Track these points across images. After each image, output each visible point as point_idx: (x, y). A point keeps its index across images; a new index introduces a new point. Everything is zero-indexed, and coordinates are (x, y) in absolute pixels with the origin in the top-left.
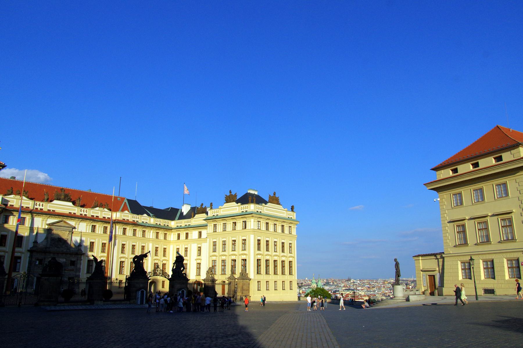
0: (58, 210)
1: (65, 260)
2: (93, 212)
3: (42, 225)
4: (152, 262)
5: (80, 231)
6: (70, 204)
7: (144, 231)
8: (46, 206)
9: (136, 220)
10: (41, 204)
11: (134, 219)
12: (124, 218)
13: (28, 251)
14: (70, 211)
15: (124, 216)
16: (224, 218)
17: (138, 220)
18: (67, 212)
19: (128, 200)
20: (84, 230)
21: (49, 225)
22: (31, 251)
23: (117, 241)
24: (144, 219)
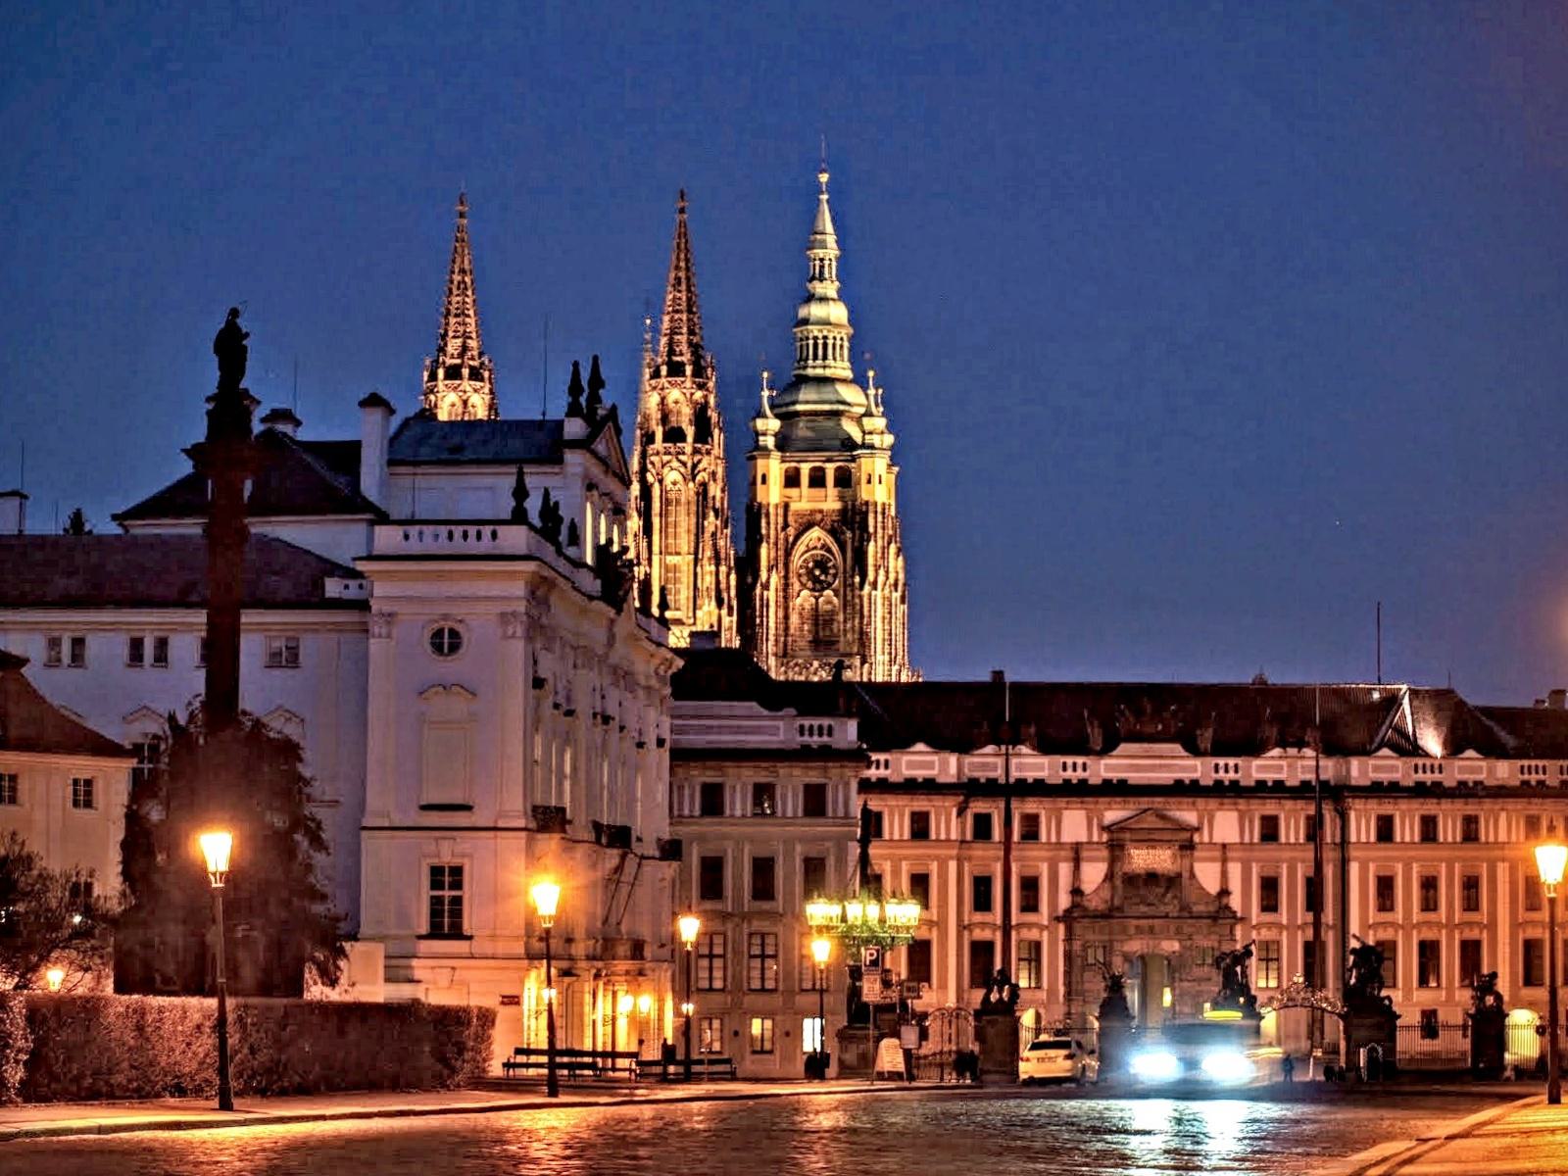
0: (1134, 778)
1: (1176, 946)
2: (1261, 768)
3: (1090, 834)
4: (1513, 936)
5: (1218, 838)
6: (1177, 748)
8: (1102, 769)
10: (1080, 760)
11: (1420, 777)
13: (1058, 919)
18: (1165, 777)
20: (1232, 837)
22: (1068, 918)
23: (1354, 869)
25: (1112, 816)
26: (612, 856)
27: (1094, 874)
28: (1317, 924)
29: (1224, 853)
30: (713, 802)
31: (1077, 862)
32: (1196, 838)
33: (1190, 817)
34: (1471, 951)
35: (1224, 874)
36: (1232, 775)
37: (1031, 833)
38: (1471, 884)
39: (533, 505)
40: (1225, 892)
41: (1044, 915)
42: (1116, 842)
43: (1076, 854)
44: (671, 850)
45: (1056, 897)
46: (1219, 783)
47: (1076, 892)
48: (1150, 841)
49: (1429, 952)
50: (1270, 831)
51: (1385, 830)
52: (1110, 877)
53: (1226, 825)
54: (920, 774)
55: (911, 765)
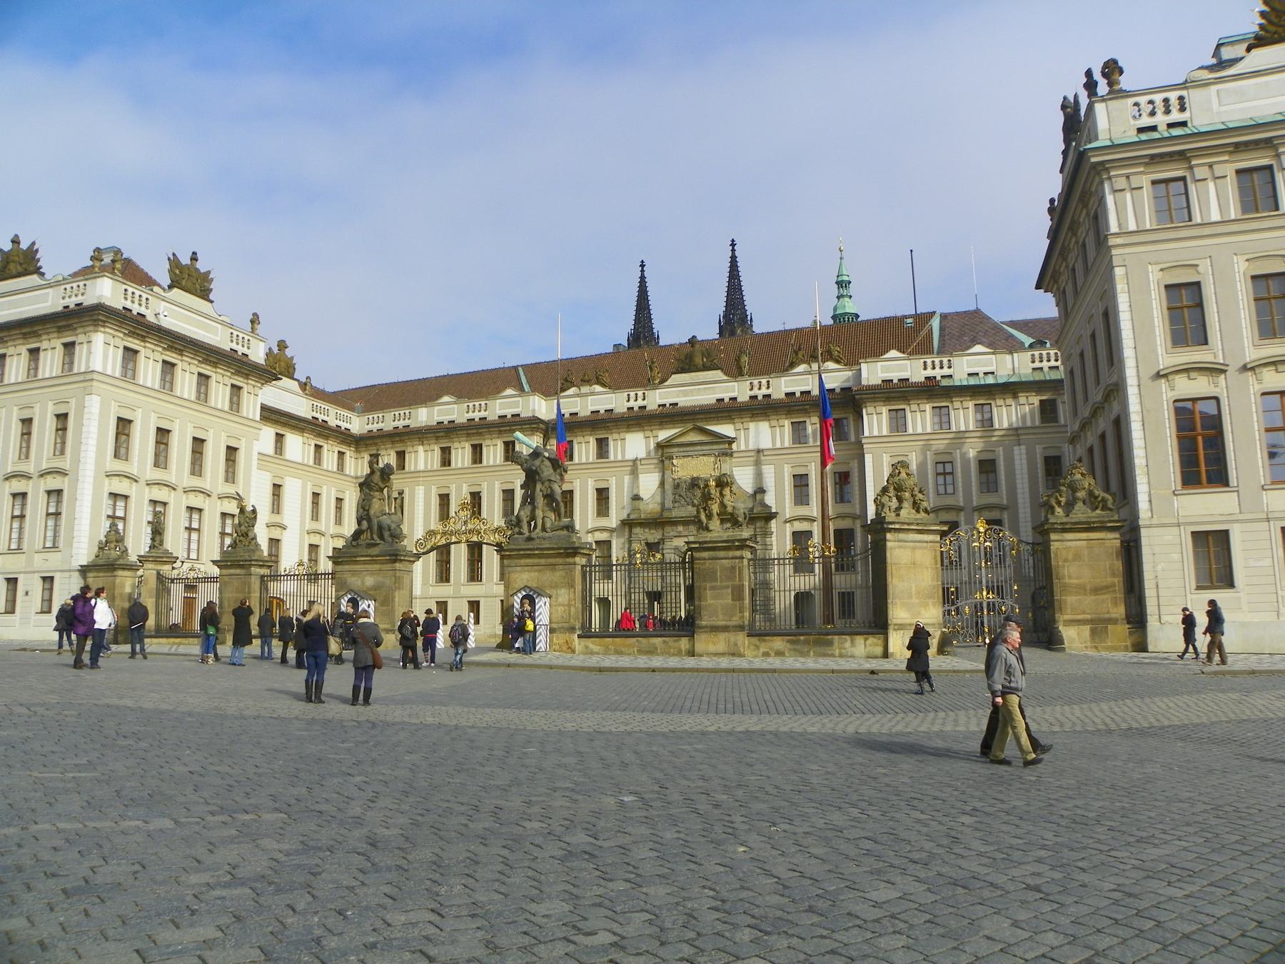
6: (718, 374)
8: (656, 398)
9: (938, 373)
11: (930, 373)
12: (888, 376)
14: (720, 396)
15: (885, 370)
17: (946, 371)
19: (944, 317)
20: (766, 443)
21: (660, 446)
23: (868, 459)
25: (664, 435)
27: (649, 484)
29: (758, 457)
31: (634, 472)
32: (734, 446)
33: (726, 429)
35: (759, 476)
36: (764, 391)
40: (760, 491)
41: (613, 521)
43: (634, 467)
46: (754, 398)
51: (898, 423)
52: (662, 484)
53: (762, 434)
54: (509, 412)
55: (502, 406)
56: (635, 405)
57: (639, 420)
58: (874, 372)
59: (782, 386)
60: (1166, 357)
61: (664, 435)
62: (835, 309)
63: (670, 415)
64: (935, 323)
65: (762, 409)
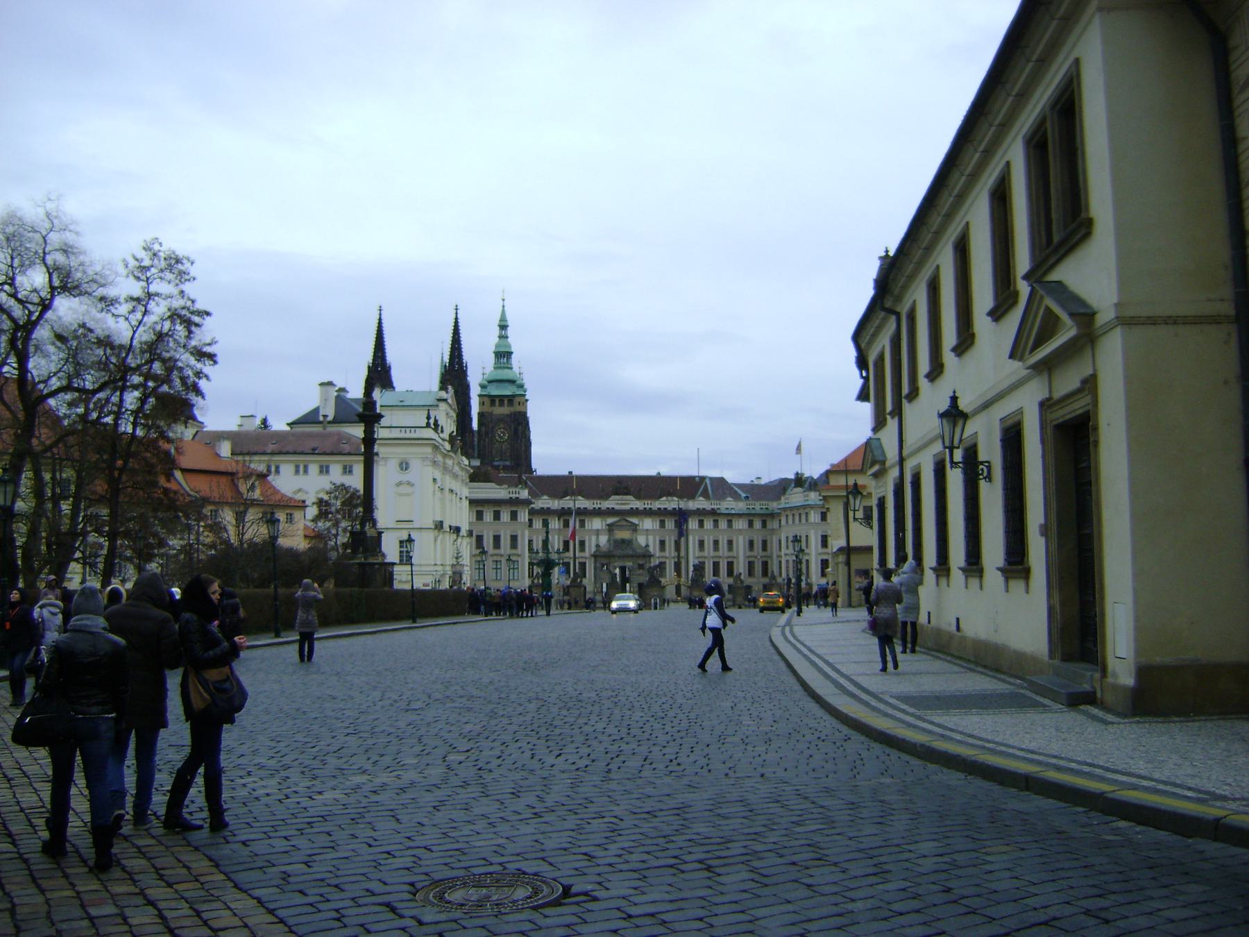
0: (617, 507)
7: (730, 522)
16: (791, 508)
18: (627, 507)
19: (711, 479)
22: (595, 556)
23: (691, 538)
24: (728, 505)
26: (454, 536)
27: (603, 539)
28: (679, 557)
30: (480, 516)
34: (730, 565)
37: (582, 523)
38: (730, 543)
39: (432, 421)
40: (647, 546)
41: (587, 554)
42: (611, 528)
43: (598, 532)
44: (470, 533)
45: (591, 548)
47: (598, 546)
48: (621, 527)
49: (716, 566)
50: (662, 524)
51: (701, 524)
53: (648, 524)
54: (545, 506)
56: (597, 506)
57: (598, 513)
58: (692, 505)
59: (657, 505)
60: (821, 550)
61: (610, 520)
62: (497, 346)
63: (611, 512)
64: (708, 481)
65: (648, 513)
